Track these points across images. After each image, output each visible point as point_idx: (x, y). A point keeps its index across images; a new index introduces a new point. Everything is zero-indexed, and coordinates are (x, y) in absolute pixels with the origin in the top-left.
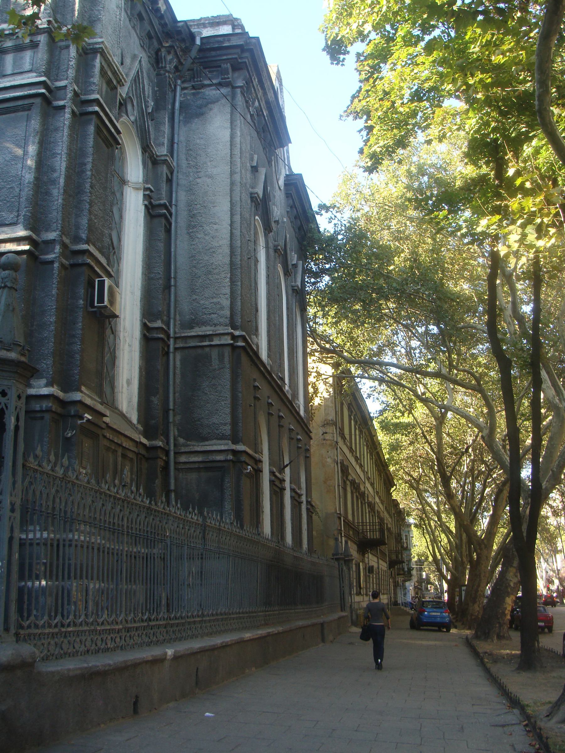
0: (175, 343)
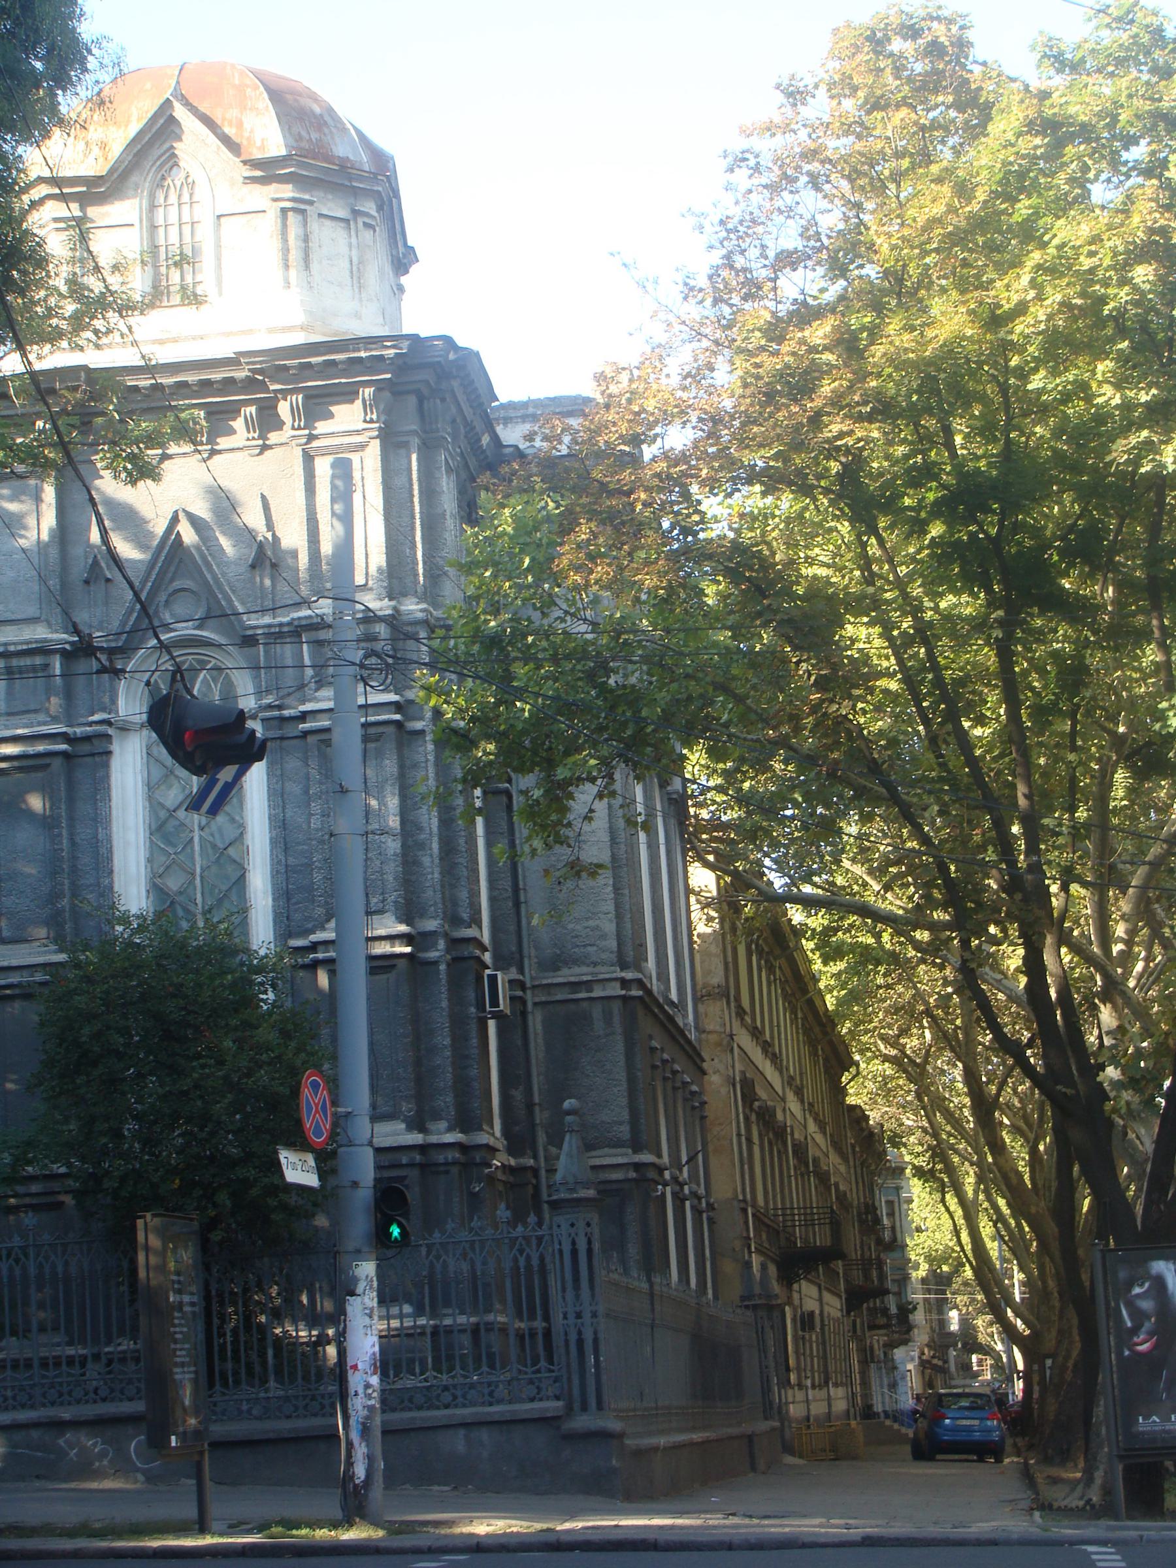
0: (533, 995)
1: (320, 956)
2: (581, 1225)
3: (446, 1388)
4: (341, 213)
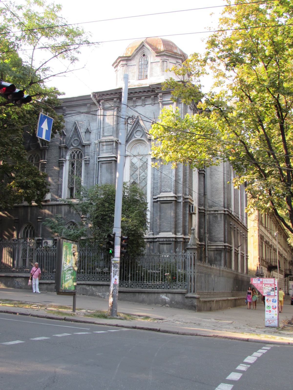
1: (158, 200)
2: (193, 253)
3: (163, 285)
4: (175, 62)
